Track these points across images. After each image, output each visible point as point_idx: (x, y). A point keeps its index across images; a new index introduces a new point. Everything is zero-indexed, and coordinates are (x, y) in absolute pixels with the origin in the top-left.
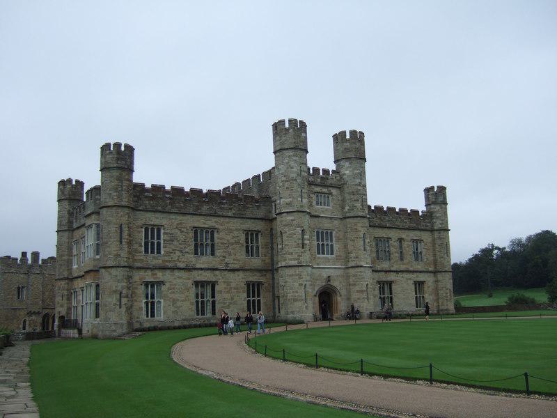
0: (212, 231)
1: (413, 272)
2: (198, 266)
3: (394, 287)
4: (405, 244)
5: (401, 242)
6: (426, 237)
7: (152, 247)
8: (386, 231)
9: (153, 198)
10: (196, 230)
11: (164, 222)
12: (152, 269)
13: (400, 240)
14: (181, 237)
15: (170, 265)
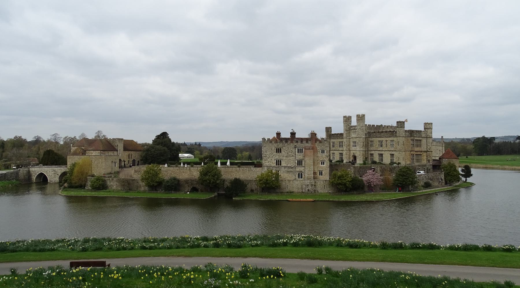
0: (342, 142)
1: (390, 151)
2: (340, 150)
3: (383, 155)
4: (387, 142)
5: (386, 141)
6: (395, 139)
7: (333, 146)
8: (382, 138)
9: (333, 137)
10: (340, 142)
11: (335, 141)
12: (333, 150)
13: (387, 141)
14: (337, 143)
15: (336, 149)
